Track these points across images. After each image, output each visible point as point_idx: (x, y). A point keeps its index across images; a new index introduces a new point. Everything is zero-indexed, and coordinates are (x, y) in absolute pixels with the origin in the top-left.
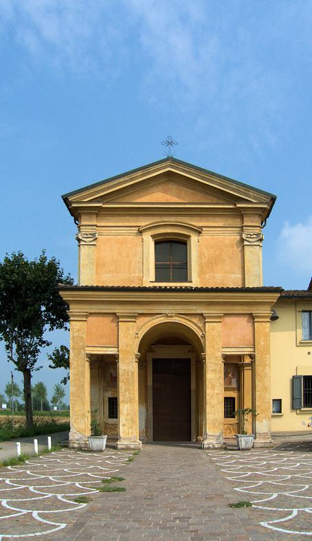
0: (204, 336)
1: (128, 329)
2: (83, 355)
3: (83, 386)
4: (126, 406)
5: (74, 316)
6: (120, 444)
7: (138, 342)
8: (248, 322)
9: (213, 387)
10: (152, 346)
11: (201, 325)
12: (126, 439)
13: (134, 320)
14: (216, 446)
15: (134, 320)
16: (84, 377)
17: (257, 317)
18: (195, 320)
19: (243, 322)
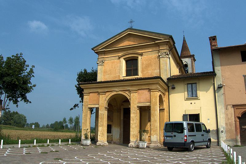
0: (130, 99)
1: (102, 97)
2: (87, 108)
3: (86, 120)
4: (101, 128)
5: (85, 94)
6: (98, 143)
7: (106, 102)
8: (148, 92)
9: (133, 121)
10: (123, 103)
11: (129, 94)
12: (100, 141)
13: (104, 94)
14: (134, 146)
15: (104, 94)
16: (87, 117)
17: (152, 89)
18: (127, 92)
19: (146, 92)
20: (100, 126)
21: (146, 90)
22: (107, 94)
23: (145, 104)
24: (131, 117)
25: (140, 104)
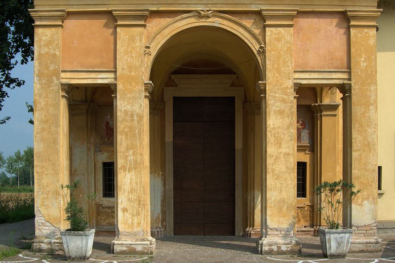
0: (262, 52)
1: (132, 39)
2: (56, 87)
3: (55, 141)
4: (129, 176)
5: (41, 18)
6: (120, 243)
7: (149, 61)
8: (339, 26)
9: (279, 144)
11: (257, 31)
12: (128, 234)
13: (142, 23)
14: (284, 248)
15: (142, 23)
16: (58, 126)
17: (356, 18)
18: (248, 23)
19: (330, 27)
20: (124, 168)
21: (329, 20)
22: (155, 24)
23: (326, 76)
24: (268, 130)
25: (307, 76)
